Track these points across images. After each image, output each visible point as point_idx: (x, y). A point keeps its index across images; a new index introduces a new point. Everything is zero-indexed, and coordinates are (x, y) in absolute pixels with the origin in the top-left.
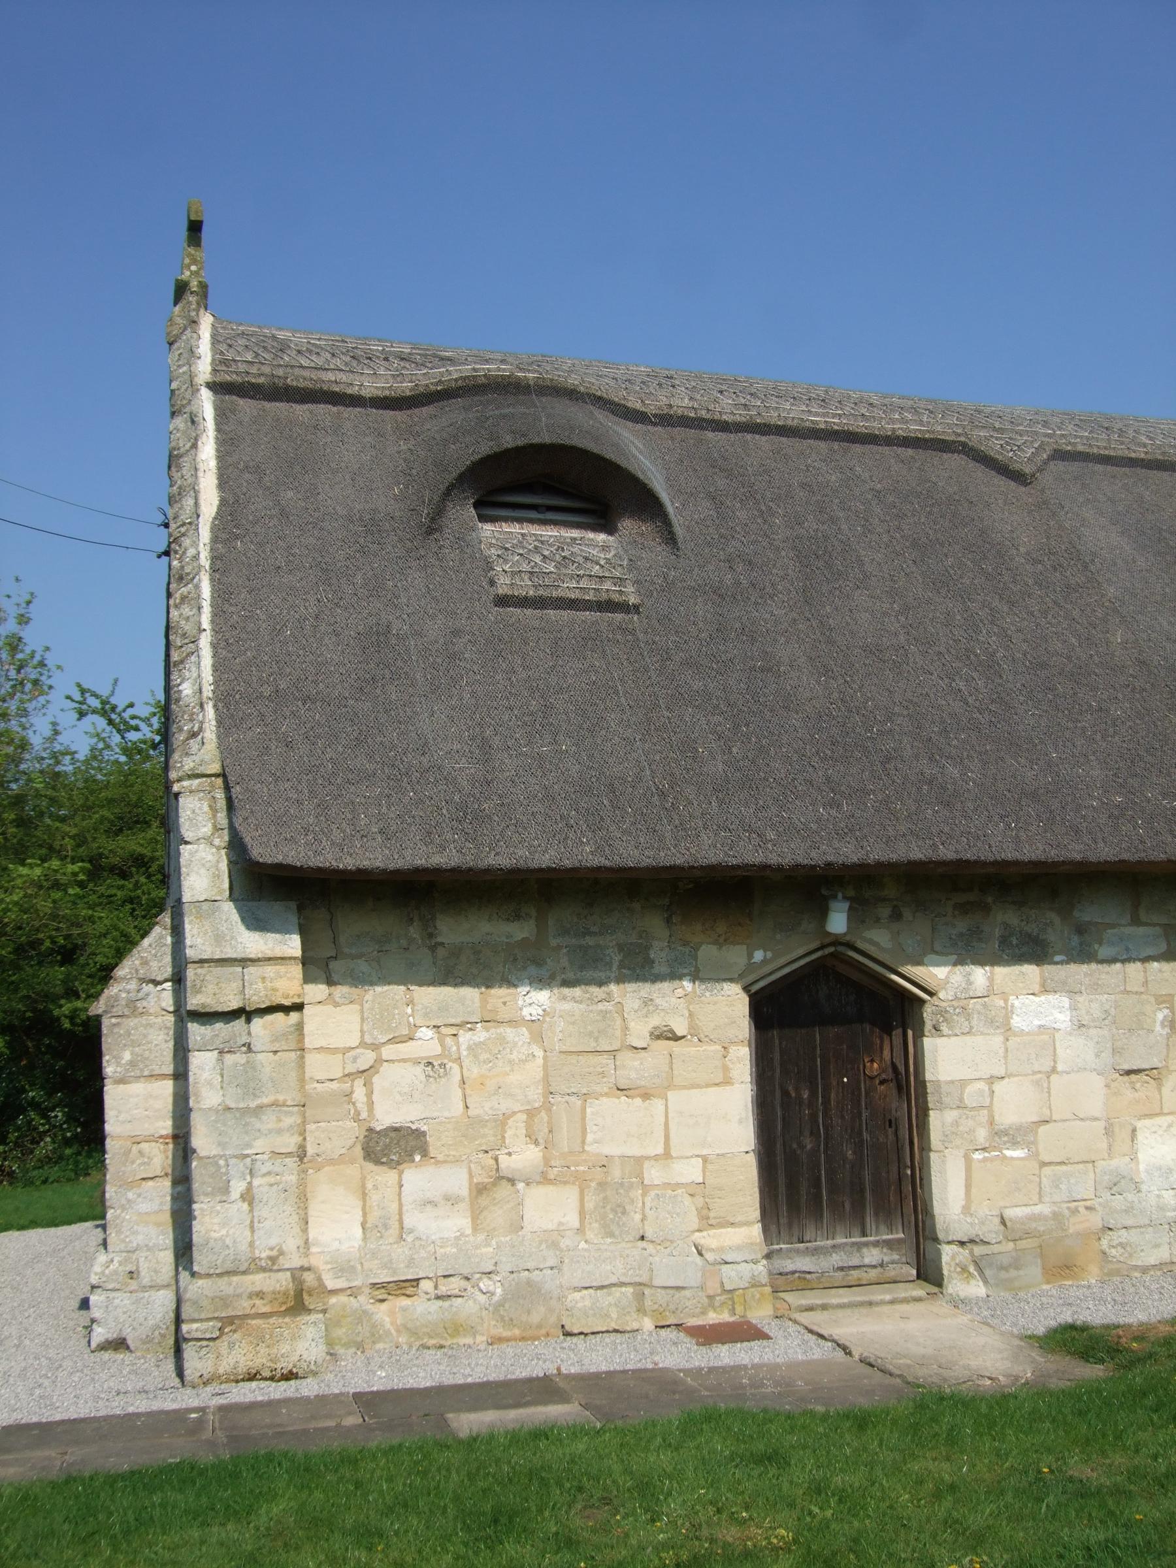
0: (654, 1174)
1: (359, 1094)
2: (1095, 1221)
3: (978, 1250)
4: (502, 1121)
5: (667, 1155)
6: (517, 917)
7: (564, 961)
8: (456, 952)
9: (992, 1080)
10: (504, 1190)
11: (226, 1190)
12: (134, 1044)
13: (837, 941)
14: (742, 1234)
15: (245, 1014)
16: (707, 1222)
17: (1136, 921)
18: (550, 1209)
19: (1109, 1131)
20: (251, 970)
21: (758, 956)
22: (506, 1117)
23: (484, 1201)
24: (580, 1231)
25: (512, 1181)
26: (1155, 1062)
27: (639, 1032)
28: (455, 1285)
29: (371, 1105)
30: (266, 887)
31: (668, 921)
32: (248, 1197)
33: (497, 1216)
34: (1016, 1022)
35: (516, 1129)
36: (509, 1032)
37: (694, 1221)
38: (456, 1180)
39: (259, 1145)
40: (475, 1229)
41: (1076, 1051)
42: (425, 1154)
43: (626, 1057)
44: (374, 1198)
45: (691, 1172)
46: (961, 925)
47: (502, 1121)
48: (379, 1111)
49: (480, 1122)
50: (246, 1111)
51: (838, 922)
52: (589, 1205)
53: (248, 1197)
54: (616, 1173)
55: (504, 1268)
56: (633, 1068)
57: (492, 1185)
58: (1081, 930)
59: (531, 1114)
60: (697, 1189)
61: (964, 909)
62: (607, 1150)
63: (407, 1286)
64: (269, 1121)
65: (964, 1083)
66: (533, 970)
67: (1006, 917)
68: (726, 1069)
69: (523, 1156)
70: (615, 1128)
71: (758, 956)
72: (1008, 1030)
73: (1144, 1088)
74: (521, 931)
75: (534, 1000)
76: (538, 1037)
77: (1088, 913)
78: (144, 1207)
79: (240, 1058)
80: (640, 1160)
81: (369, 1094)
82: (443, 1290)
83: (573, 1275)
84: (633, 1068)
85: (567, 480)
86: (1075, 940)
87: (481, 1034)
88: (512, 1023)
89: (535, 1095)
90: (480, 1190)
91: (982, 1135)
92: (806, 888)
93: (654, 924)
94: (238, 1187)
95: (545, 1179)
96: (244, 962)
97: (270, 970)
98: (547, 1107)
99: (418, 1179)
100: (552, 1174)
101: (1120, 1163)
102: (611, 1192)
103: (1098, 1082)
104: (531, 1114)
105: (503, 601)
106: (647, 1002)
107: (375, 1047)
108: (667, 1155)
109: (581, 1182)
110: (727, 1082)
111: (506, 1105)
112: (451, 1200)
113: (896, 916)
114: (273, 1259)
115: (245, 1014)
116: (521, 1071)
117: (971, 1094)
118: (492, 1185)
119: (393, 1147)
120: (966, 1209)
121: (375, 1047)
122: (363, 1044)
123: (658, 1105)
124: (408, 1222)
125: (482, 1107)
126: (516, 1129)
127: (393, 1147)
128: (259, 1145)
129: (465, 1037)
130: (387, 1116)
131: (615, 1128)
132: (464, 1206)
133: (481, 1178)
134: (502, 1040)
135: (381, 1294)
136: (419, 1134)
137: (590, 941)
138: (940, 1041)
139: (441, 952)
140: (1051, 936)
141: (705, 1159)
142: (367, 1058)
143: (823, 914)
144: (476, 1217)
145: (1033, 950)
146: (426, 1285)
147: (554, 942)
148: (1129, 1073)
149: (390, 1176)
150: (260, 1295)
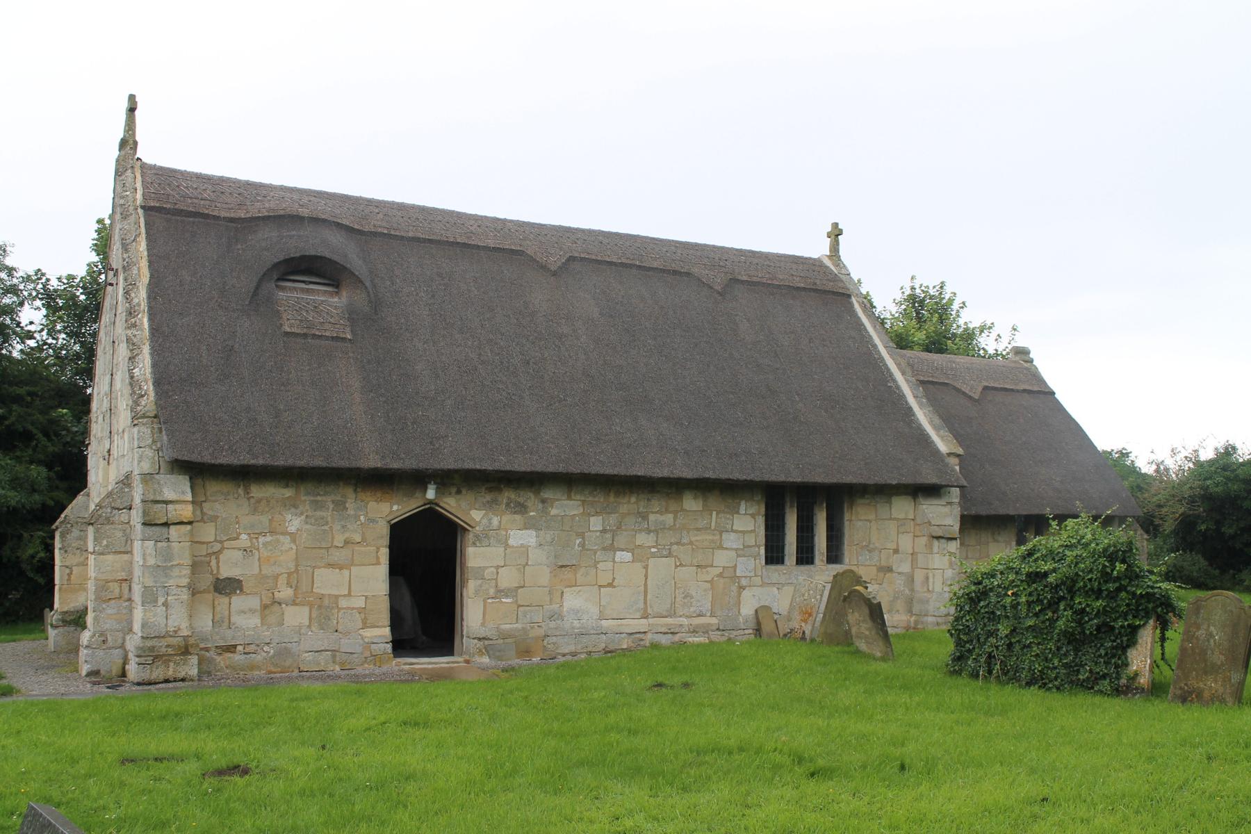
0: (343, 603)
1: (213, 563)
2: (541, 632)
3: (486, 642)
4: (276, 577)
5: (349, 595)
6: (287, 486)
7: (307, 507)
8: (259, 501)
9: (498, 567)
10: (276, 607)
11: (156, 601)
12: (108, 537)
13: (430, 502)
15: (166, 524)
16: (365, 626)
17: (569, 498)
18: (297, 616)
19: (550, 593)
20: (170, 507)
21: (395, 508)
22: (278, 575)
23: (267, 612)
24: (309, 626)
25: (280, 604)
27: (339, 540)
28: (252, 648)
29: (218, 567)
31: (355, 490)
32: (165, 604)
34: (511, 542)
35: (282, 580)
36: (281, 538)
38: (254, 602)
39: (171, 582)
40: (262, 624)
41: (536, 555)
42: (241, 590)
44: (218, 609)
45: (360, 603)
46: (488, 497)
47: (276, 577)
48: (222, 571)
49: (267, 577)
50: (166, 568)
51: (431, 494)
52: (314, 616)
53: (165, 604)
54: (326, 602)
56: (337, 556)
57: (270, 606)
58: (543, 501)
59: (289, 574)
60: (361, 611)
61: (490, 490)
63: (231, 649)
64: (176, 572)
66: (293, 510)
67: (509, 494)
68: (378, 558)
69: (285, 593)
70: (327, 582)
71: (395, 508)
72: (507, 546)
73: (567, 574)
74: (288, 493)
75: (294, 523)
76: (294, 541)
77: (547, 494)
78: (109, 611)
79: (165, 544)
80: (337, 597)
81: (218, 563)
82: (247, 650)
84: (337, 556)
86: (540, 506)
87: (269, 538)
88: (282, 534)
89: (292, 566)
90: (265, 607)
91: (492, 591)
92: (418, 479)
93: (349, 491)
94: (161, 600)
95: (294, 603)
96: (166, 502)
97: (178, 506)
98: (297, 571)
99: (237, 601)
100: (298, 601)
101: (555, 607)
102: (323, 609)
103: (547, 570)
104: (289, 574)
106: (343, 527)
107: (221, 542)
108: (349, 595)
109: (311, 606)
110: (378, 563)
111: (277, 570)
112: (252, 611)
113: (459, 492)
114: (175, 632)
116: (286, 553)
117: (489, 573)
118: (270, 606)
119: (226, 587)
120: (483, 624)
121: (221, 542)
122: (216, 541)
123: (346, 572)
124: (233, 620)
125: (267, 571)
126: (282, 580)
127: (226, 587)
128: (171, 582)
129: (261, 539)
130: (225, 573)
131: (327, 582)
132: (258, 614)
133: (267, 601)
134: (278, 541)
135: (219, 651)
136: (239, 582)
137: (319, 498)
139: (252, 501)
140: (529, 504)
141: (366, 597)
142: (217, 547)
143: (425, 489)
144: (263, 618)
145: (521, 509)
146: (240, 648)
147: (303, 498)
148: (562, 566)
149: (226, 600)
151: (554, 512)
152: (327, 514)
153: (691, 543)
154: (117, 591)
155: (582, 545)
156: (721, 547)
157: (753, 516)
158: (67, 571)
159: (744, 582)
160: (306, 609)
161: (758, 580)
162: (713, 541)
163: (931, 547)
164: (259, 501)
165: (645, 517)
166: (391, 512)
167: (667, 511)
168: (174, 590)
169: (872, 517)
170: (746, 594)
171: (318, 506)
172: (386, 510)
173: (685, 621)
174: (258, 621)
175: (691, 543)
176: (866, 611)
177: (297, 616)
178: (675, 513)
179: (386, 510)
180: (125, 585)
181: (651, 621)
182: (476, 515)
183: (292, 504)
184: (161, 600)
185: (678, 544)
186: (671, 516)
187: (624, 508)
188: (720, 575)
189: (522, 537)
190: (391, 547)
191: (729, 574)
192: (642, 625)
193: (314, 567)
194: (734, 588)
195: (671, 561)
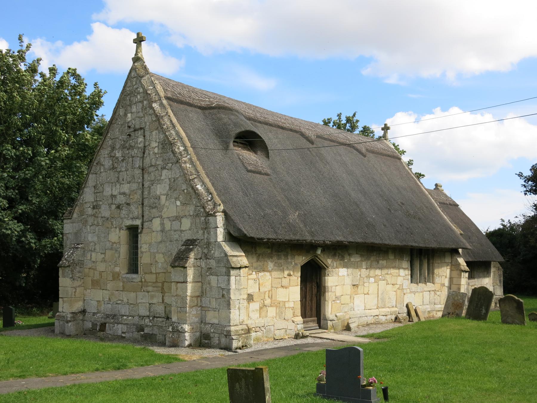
0: (287, 305)
3: (334, 322)
4: (265, 293)
5: (289, 301)
10: (265, 308)
14: (300, 319)
16: (294, 316)
17: (357, 254)
26: (358, 283)
30: (237, 239)
33: (263, 314)
37: (292, 315)
43: (283, 279)
47: (265, 293)
51: (319, 252)
53: (239, 309)
54: (281, 304)
55: (266, 325)
59: (269, 291)
62: (281, 300)
65: (332, 287)
69: (268, 301)
70: (281, 295)
71: (304, 258)
77: (351, 252)
80: (285, 302)
83: (277, 327)
85: (249, 140)
90: (261, 308)
91: (334, 297)
95: (271, 306)
103: (350, 287)
104: (269, 291)
105: (249, 171)
108: (289, 301)
109: (276, 306)
115: (240, 268)
131: (281, 295)
137: (279, 254)
138: (329, 278)
145: (343, 258)
146: (254, 329)
148: (354, 285)
150: (242, 330)
151: (352, 259)
152: (282, 261)
153: (391, 274)
154: (196, 302)
155: (360, 275)
156: (399, 276)
157: (407, 261)
158: (74, 290)
159: (405, 291)
160: (275, 308)
161: (408, 291)
162: (397, 273)
163: (461, 275)
164: (259, 256)
165: (378, 262)
166: (303, 260)
167: (384, 260)
168: (242, 301)
169: (439, 262)
170: (405, 296)
171: (279, 258)
172: (302, 260)
173: (388, 310)
174: (258, 315)
175: (391, 274)
176: (515, 305)
177: (272, 311)
178: (386, 260)
179: (302, 260)
180: (199, 299)
181: (380, 309)
182: (329, 261)
183: (270, 256)
184: (237, 306)
185: (387, 274)
186: (385, 261)
187: (372, 259)
188: (399, 289)
189: (343, 271)
190: (301, 277)
191: (401, 288)
192: (376, 312)
193: (277, 288)
194: (402, 294)
195: (384, 282)
